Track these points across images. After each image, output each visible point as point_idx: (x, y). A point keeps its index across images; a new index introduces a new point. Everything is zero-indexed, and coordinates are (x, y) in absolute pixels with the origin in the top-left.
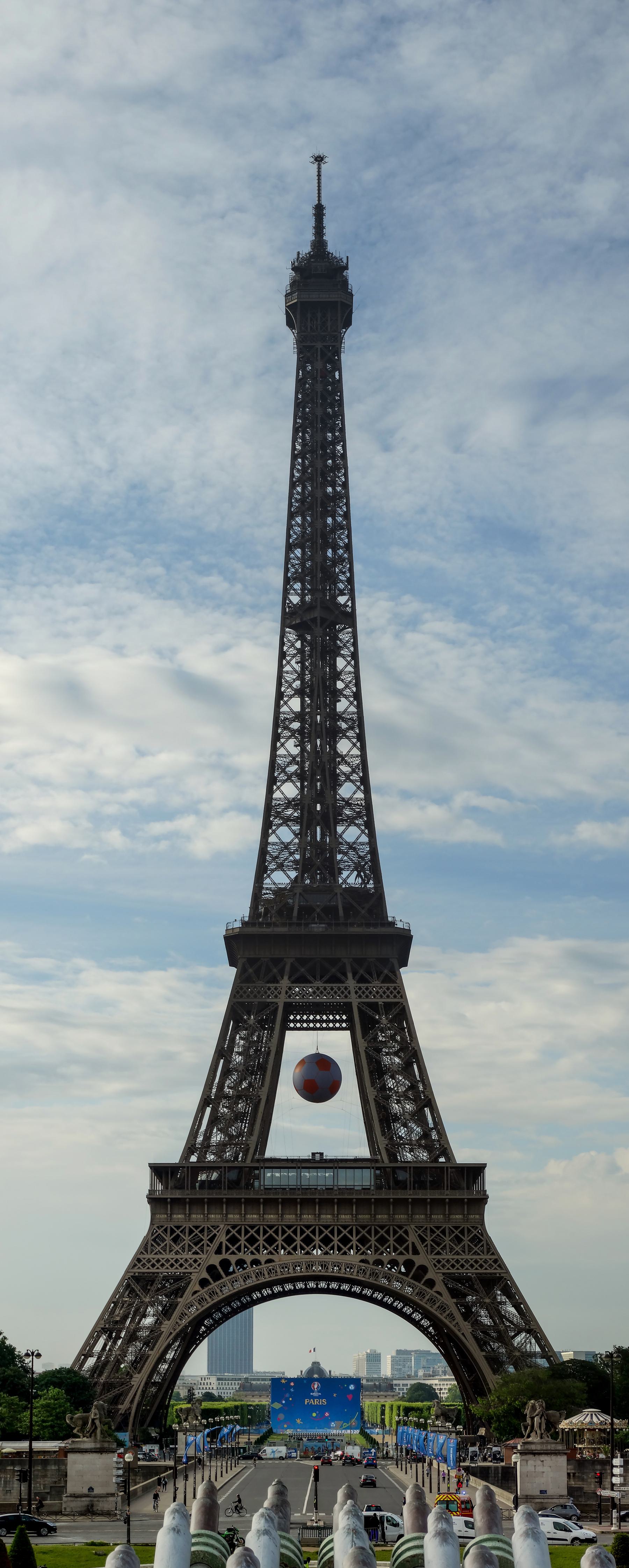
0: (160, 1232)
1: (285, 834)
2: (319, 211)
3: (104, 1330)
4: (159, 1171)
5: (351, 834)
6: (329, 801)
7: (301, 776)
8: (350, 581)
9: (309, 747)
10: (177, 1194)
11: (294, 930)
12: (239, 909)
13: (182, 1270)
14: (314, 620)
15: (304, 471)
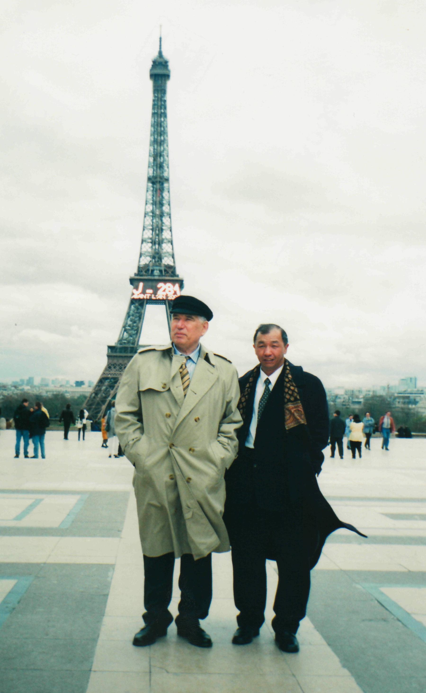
0: (110, 365)
1: (147, 247)
2: (160, 39)
3: (94, 393)
4: (111, 348)
5: (166, 247)
6: (160, 239)
7: (152, 230)
8: (168, 167)
9: (154, 221)
10: (115, 354)
11: (150, 277)
12: (132, 271)
13: (116, 376)
14: (157, 182)
15: (154, 131)
